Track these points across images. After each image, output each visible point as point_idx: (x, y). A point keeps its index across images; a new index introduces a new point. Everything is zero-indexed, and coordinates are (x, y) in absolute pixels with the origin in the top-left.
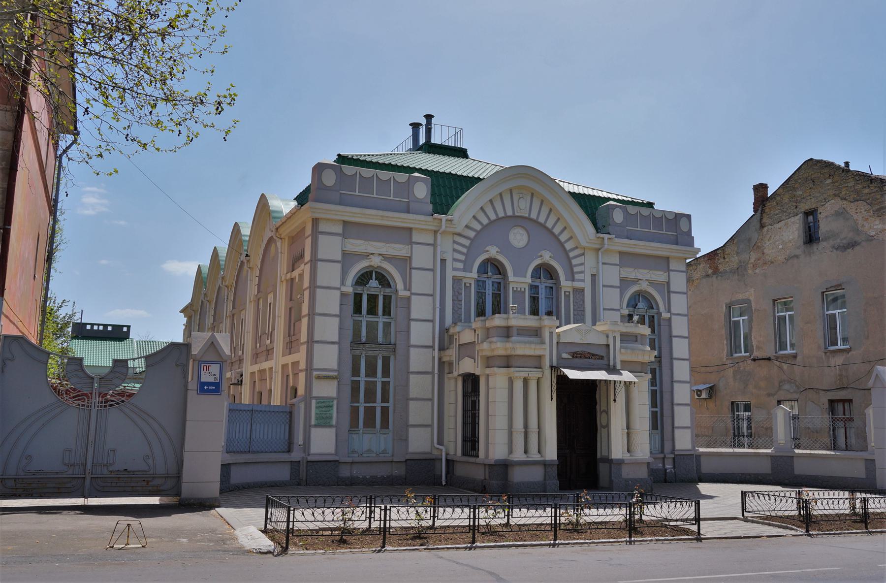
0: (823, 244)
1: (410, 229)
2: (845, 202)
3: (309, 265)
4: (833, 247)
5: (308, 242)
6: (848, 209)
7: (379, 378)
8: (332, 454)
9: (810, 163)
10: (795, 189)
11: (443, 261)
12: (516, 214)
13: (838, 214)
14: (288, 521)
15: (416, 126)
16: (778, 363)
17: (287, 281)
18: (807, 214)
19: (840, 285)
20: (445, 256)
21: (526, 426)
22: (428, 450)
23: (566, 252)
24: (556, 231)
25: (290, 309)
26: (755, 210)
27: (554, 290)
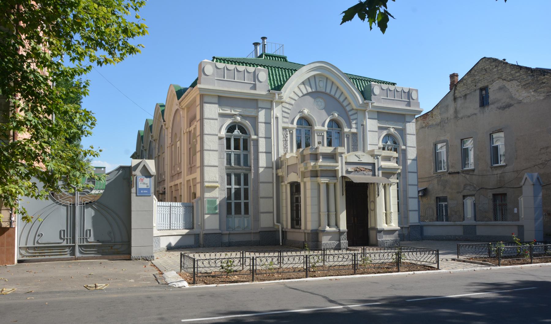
0: (491, 106)
1: (257, 100)
2: (505, 81)
3: (199, 122)
4: (497, 108)
5: (198, 109)
6: (506, 85)
7: (242, 187)
8: (216, 230)
9: (484, 60)
10: (474, 75)
11: (277, 118)
13: (500, 89)
14: (194, 268)
15: (256, 44)
16: (464, 175)
17: (187, 133)
18: (481, 89)
19: (501, 129)
21: (328, 211)
22: (271, 225)
25: (190, 149)
26: (451, 89)
27: (340, 133)
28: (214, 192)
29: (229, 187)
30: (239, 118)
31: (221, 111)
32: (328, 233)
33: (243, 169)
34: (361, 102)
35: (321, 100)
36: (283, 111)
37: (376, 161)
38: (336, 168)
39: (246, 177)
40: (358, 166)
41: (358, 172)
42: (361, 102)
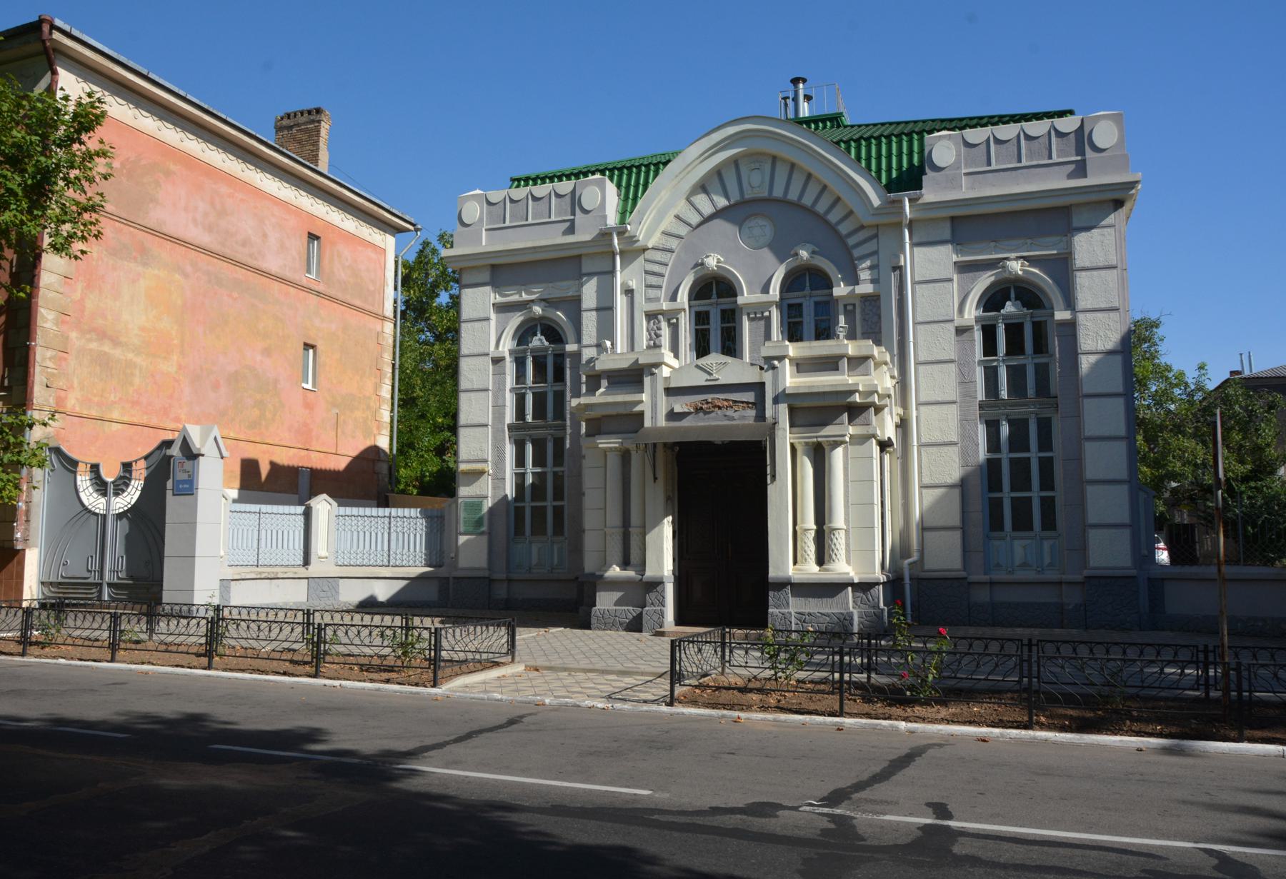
1: (579, 257)
7: (550, 468)
12: (747, 197)
20: (633, 284)
23: (841, 239)
24: (821, 208)
28: (477, 484)
29: (521, 470)
30: (538, 310)
31: (499, 299)
32: (615, 584)
33: (550, 427)
34: (876, 202)
35: (761, 221)
36: (647, 272)
37: (767, 377)
38: (638, 408)
39: (559, 442)
40: (709, 397)
41: (706, 413)
42: (876, 202)
